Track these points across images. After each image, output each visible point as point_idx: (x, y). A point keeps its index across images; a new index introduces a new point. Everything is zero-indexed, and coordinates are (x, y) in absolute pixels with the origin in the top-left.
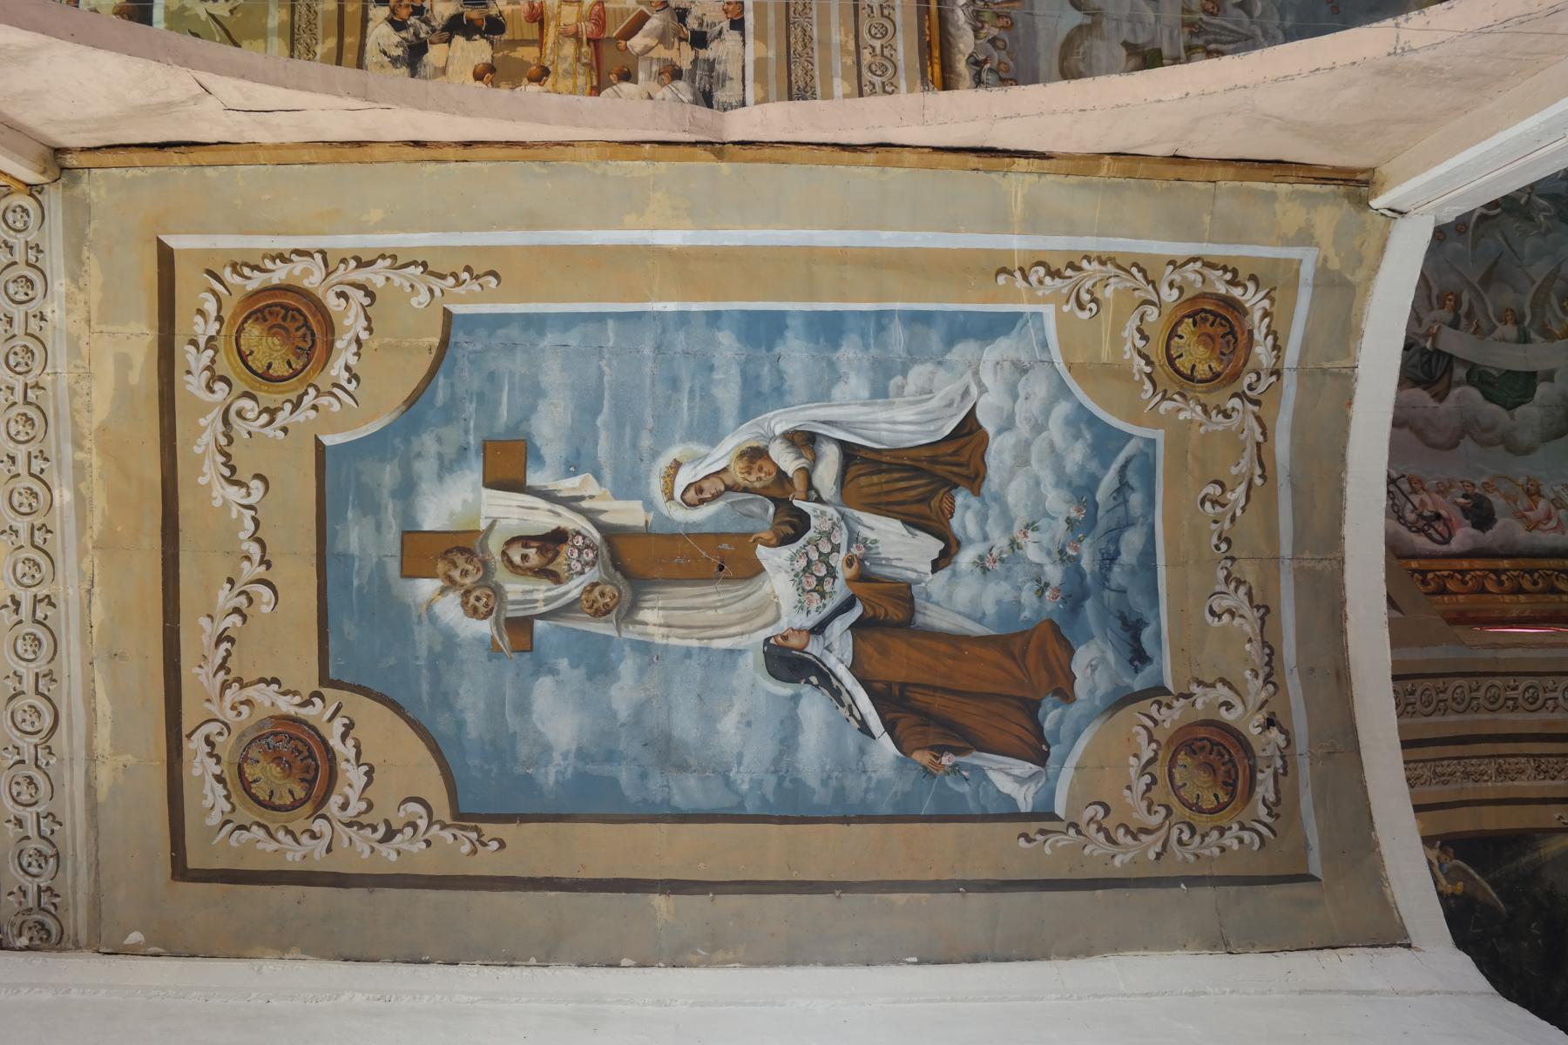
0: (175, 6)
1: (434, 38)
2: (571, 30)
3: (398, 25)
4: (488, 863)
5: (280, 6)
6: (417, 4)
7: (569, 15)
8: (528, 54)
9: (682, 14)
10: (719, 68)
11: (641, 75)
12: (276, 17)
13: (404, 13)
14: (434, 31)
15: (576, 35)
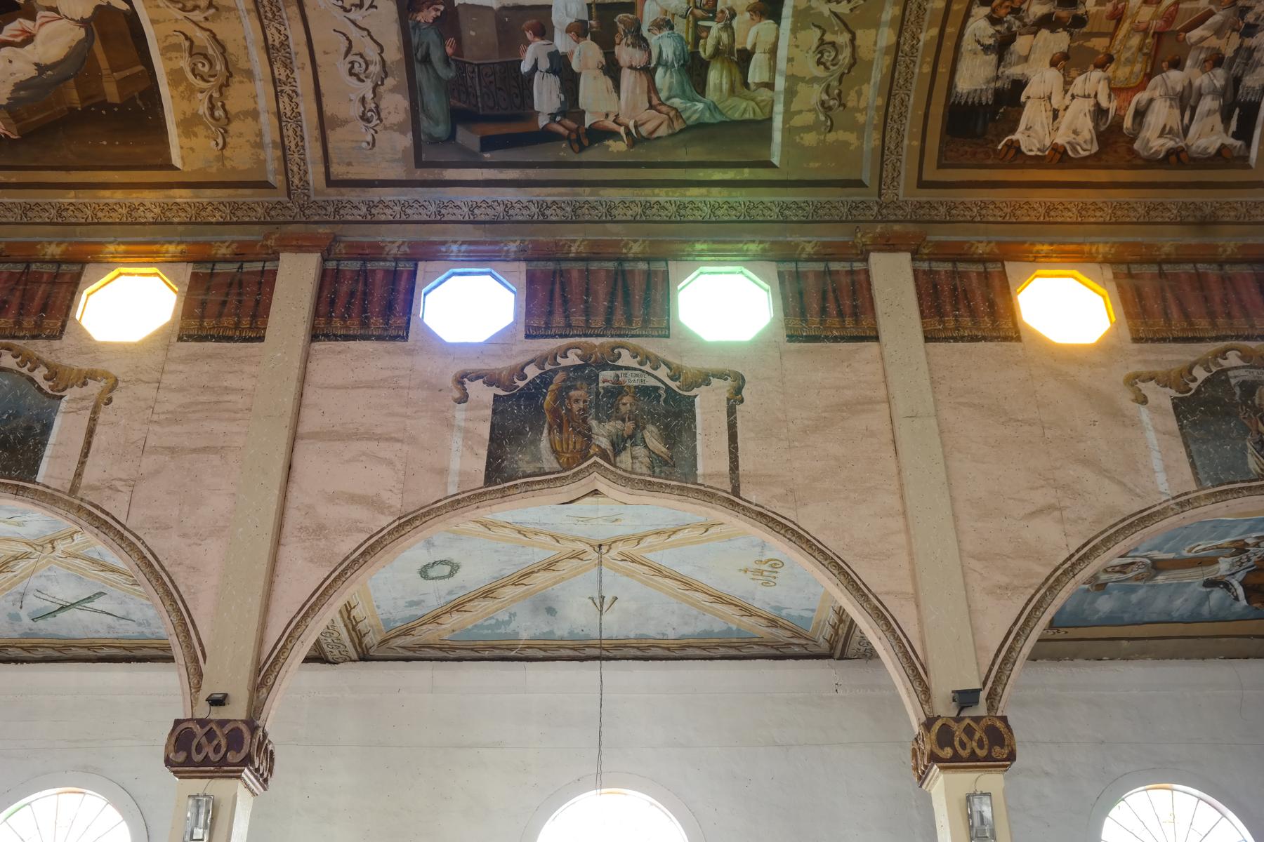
0: (803, 5)
1: (1023, 31)
2: (1143, 26)
3: (993, 20)
4: (1057, 636)
5: (895, 4)
6: (1016, 5)
7: (1146, 13)
8: (1099, 44)
9: (1245, 10)
10: (1257, 55)
11: (1189, 63)
12: (890, 12)
13: (1002, 12)
14: (1025, 25)
15: (1145, 32)
